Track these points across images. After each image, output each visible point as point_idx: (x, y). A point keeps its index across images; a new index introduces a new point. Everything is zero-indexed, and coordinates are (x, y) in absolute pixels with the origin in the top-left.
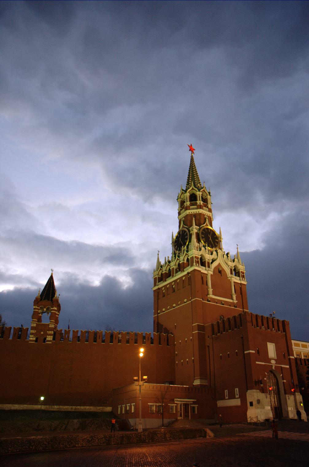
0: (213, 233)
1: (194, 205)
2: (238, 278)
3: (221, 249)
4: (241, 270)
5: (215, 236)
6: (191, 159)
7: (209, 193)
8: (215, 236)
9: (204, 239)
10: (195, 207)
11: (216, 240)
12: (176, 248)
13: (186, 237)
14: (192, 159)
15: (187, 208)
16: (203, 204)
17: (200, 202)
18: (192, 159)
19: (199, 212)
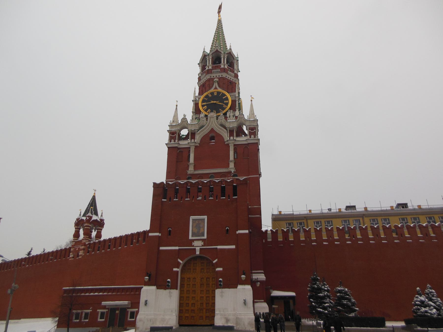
12: (204, 108)
13: (225, 102)
15: (224, 70)
18: (220, 22)
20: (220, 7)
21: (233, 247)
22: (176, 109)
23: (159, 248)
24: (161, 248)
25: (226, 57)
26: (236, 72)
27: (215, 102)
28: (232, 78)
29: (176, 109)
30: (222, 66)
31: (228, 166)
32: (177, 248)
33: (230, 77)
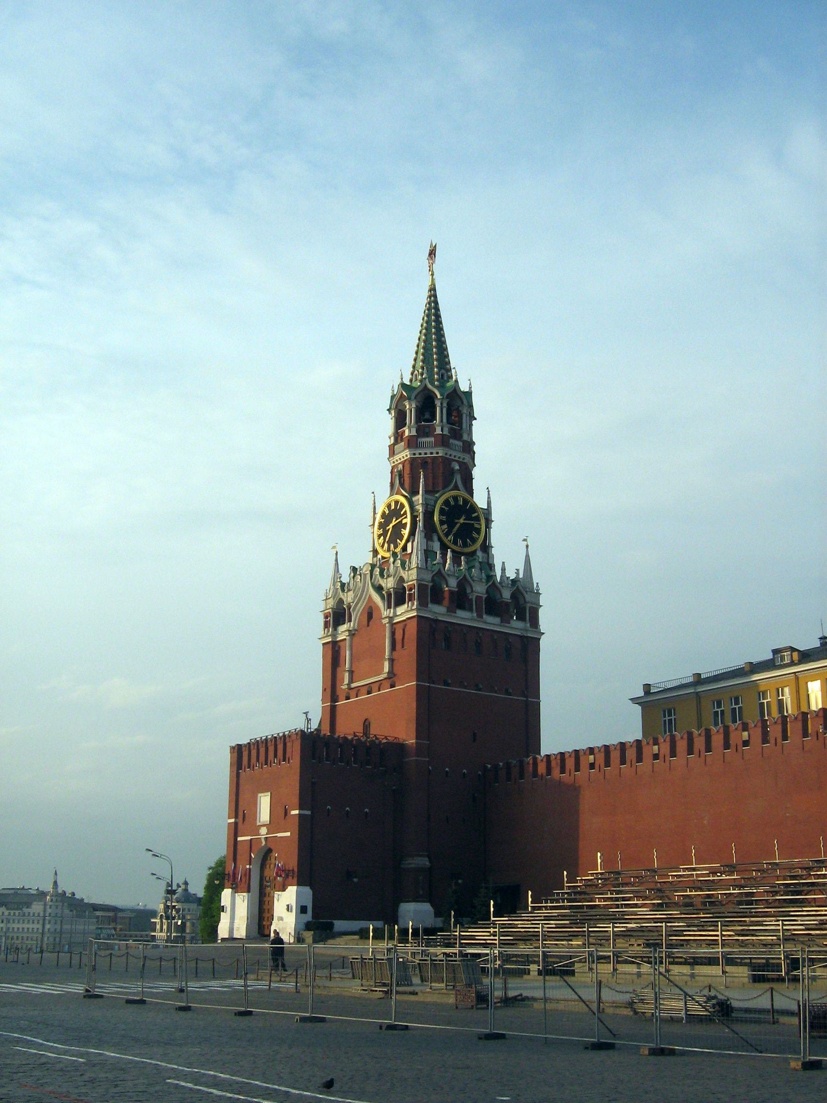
0: (474, 508)
1: (427, 435)
2: (520, 625)
3: (486, 548)
4: (528, 605)
5: (474, 515)
6: (430, 290)
7: (469, 394)
8: (474, 515)
9: (445, 526)
10: (433, 439)
11: (476, 526)
13: (404, 522)
14: (433, 289)
15: (412, 443)
16: (451, 430)
17: (439, 426)
19: (437, 453)
20: (432, 253)
21: (288, 834)
22: (336, 560)
23: (236, 839)
24: (239, 839)
25: (414, 406)
26: (438, 431)
27: (391, 526)
28: (428, 451)
29: (336, 560)
30: (407, 434)
31: (381, 672)
32: (249, 838)
33: (423, 452)
